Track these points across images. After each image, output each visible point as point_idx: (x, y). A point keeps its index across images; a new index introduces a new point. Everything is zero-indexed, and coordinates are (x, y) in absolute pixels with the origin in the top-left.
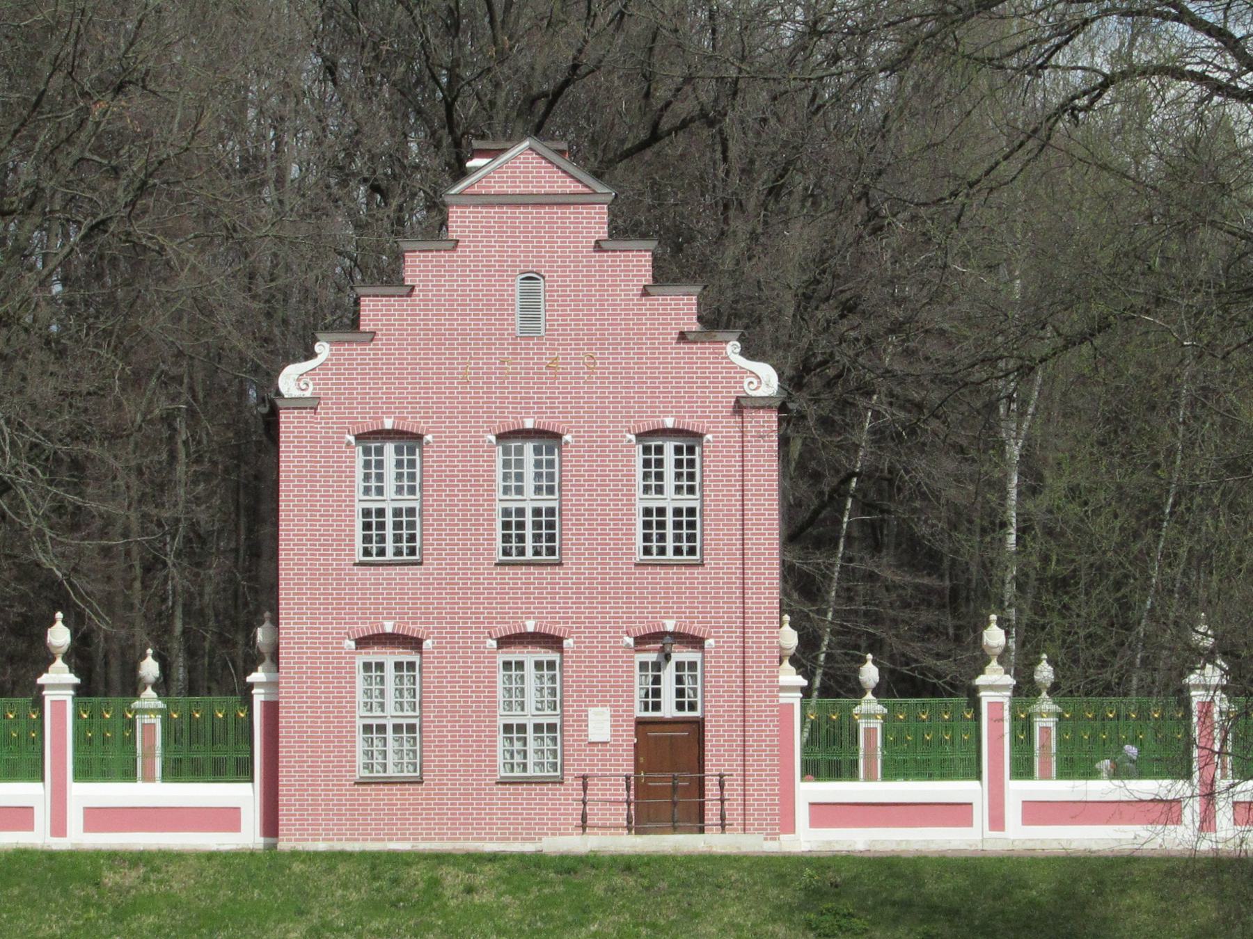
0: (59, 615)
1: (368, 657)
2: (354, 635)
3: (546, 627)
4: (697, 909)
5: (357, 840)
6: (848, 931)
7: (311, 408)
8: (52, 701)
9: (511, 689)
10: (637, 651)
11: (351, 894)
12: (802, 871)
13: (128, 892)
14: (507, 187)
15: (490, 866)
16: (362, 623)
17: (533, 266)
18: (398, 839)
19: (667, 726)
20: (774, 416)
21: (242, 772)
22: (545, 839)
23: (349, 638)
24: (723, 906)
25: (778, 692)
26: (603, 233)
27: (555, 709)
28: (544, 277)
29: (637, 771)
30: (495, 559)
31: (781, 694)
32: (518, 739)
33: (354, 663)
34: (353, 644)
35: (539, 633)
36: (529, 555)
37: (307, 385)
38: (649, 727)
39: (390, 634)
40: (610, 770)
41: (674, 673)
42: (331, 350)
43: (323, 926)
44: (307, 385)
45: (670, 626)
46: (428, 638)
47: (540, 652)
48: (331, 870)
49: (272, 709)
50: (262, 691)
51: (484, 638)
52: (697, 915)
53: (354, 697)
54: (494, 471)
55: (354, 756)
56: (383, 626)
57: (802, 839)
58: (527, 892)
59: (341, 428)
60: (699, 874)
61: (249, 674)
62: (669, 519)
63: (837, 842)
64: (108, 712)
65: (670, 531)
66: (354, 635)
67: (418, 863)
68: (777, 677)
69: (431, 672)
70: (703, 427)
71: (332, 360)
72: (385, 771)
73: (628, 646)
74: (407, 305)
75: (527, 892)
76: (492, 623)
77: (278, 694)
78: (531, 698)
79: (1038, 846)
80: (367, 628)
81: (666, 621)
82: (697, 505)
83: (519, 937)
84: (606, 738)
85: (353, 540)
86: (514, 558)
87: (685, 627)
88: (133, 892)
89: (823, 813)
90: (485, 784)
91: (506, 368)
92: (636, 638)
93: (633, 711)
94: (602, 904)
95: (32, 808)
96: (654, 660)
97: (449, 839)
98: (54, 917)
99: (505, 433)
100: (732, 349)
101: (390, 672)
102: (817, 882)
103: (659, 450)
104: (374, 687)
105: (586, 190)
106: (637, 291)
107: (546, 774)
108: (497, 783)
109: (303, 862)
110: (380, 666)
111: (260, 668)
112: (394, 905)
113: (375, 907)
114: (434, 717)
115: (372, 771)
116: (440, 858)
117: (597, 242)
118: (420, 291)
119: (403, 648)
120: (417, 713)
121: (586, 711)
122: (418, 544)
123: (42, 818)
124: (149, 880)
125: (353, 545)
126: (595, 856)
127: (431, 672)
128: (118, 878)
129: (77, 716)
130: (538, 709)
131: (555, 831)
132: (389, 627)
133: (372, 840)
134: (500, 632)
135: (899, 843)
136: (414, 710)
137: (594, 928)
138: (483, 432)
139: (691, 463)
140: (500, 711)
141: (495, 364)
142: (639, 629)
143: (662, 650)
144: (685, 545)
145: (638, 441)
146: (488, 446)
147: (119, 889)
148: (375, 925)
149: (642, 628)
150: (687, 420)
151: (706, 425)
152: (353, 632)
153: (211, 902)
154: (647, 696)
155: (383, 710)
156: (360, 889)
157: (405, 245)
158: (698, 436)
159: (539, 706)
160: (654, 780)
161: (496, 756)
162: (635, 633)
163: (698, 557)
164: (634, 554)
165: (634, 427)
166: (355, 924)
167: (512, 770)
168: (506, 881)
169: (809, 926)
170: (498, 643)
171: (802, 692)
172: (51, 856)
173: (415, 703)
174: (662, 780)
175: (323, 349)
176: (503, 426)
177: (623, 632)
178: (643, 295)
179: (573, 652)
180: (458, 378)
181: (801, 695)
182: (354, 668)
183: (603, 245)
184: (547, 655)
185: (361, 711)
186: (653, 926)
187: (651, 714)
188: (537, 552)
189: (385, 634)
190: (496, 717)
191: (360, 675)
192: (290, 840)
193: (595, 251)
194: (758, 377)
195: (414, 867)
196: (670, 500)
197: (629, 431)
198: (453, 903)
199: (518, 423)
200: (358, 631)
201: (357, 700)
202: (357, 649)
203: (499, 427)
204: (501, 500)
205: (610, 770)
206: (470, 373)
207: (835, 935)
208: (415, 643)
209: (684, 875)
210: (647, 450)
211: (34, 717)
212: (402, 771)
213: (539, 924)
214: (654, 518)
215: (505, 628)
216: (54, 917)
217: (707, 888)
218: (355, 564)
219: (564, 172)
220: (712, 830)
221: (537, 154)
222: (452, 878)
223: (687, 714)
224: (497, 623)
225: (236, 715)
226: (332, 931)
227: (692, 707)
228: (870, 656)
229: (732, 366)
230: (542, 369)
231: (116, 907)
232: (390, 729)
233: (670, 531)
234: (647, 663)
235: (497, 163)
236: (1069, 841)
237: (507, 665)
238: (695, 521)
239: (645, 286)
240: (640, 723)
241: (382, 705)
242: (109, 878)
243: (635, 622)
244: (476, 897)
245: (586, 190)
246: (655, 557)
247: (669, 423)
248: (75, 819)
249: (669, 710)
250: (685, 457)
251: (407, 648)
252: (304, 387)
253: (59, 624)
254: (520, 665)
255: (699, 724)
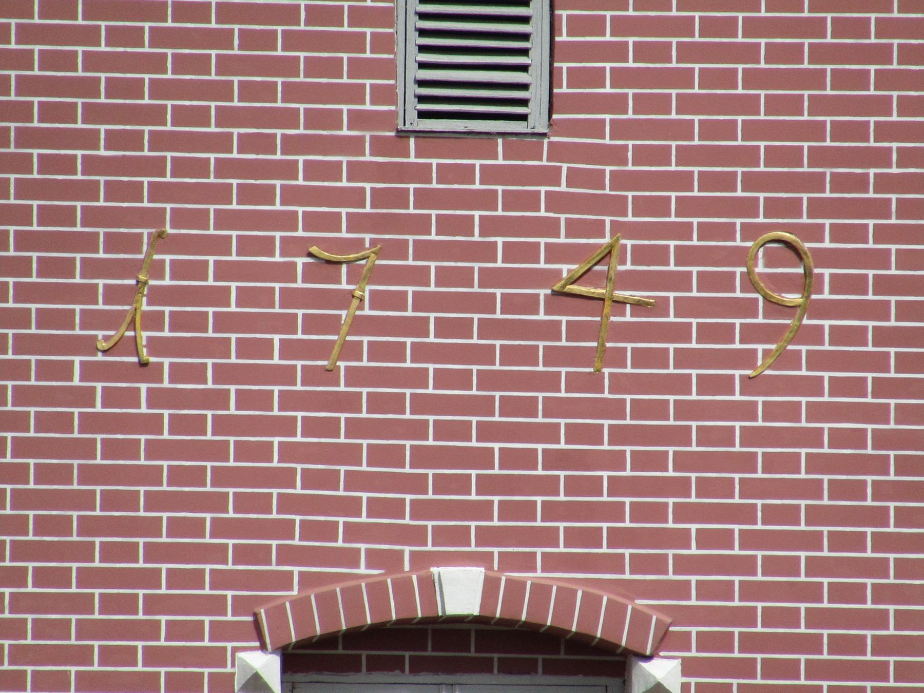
91: (343, 300)
99: (329, 640)
138: (219, 632)
141: (286, 271)
176: (326, 601)
180: (87, 345)
199: (403, 588)
203: (301, 605)
206: (154, 321)
230: (531, 305)
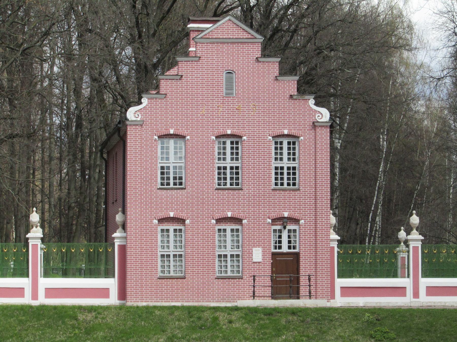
0: (35, 209)
1: (163, 227)
2: (215, 218)
3: (236, 215)
4: (324, 329)
5: (159, 301)
6: (388, 338)
7: (140, 125)
8: (413, 247)
9: (221, 240)
10: (272, 225)
11: (182, 323)
12: (364, 314)
13: (90, 323)
14: (220, 35)
15: (236, 312)
16: (161, 213)
17: (230, 68)
18: (175, 301)
19: (284, 256)
20: (328, 130)
21: (109, 274)
22: (238, 301)
23: (156, 219)
24: (335, 328)
25: (330, 242)
26: (259, 54)
27: (239, 248)
28: (235, 72)
29: (272, 273)
30: (215, 187)
31: (331, 243)
32: (224, 261)
33: (157, 229)
34: (157, 221)
35: (233, 217)
36: (228, 186)
37: (138, 115)
38: (277, 256)
39: (172, 217)
40: (262, 273)
41: (287, 234)
42: (148, 101)
43: (173, 336)
44: (138, 115)
45: (286, 215)
46: (188, 219)
47: (233, 225)
48: (172, 314)
49: (123, 249)
50: (118, 241)
51: (211, 219)
52: (324, 332)
53: (157, 243)
54: (215, 151)
55: (157, 268)
56: (169, 214)
57: (338, 302)
58: (254, 322)
59: (152, 133)
60: (322, 316)
61: (113, 234)
62: (285, 171)
63: (352, 303)
64: (64, 249)
65: (285, 176)
66: (157, 218)
67: (207, 310)
68: (329, 236)
69: (189, 233)
70: (299, 134)
71: (148, 105)
72: (169, 273)
73: (269, 223)
74: (179, 83)
75: (254, 322)
76: (214, 213)
77: (127, 242)
78: (229, 244)
79: (433, 304)
80: (163, 215)
81: (284, 213)
82: (296, 165)
83: (254, 341)
84: (260, 260)
85: (157, 179)
86: (222, 187)
87: (292, 215)
88: (92, 322)
89: (346, 291)
90: (211, 279)
91: (220, 109)
92: (272, 220)
93: (271, 249)
94: (286, 328)
95: (24, 288)
96: (279, 229)
97: (196, 301)
98: (61, 333)
99: (219, 136)
100: (312, 102)
101: (171, 233)
102: (372, 319)
103: (281, 143)
104: (165, 239)
105: (252, 37)
106: (272, 78)
107: (235, 275)
108: (216, 279)
109: (159, 310)
110: (168, 231)
111: (117, 231)
112: (201, 328)
113: (193, 329)
114: (190, 251)
115: (164, 274)
116: (216, 309)
117: (257, 58)
118: (185, 77)
119: (177, 223)
120: (183, 250)
121: (252, 249)
122: (240, 181)
123: (28, 292)
124: (98, 317)
125: (157, 181)
126: (278, 308)
127: (189, 233)
128: (84, 317)
129: (423, 253)
130: (232, 248)
131: (239, 298)
132: (172, 215)
133: (165, 302)
134: (217, 217)
135: (377, 303)
136: (181, 249)
137: (284, 337)
139: (237, 149)
140: (217, 249)
142: (274, 216)
143: (283, 224)
144: (291, 182)
145: (273, 139)
146: (212, 141)
147: (85, 321)
148: (194, 336)
149: (274, 215)
150: (293, 131)
151: (301, 133)
152: (157, 217)
153: (125, 326)
154: (276, 243)
155: (169, 249)
156: (185, 321)
157: (178, 59)
158: (240, 137)
159: (232, 247)
160: (279, 277)
161: (215, 267)
162: (272, 217)
163: (297, 187)
164: (271, 185)
165: (271, 134)
166: (186, 335)
167: (221, 273)
168: (245, 318)
169: (371, 336)
170: (158, 221)
171: (422, 242)
172: (31, 307)
173: (182, 246)
174: (285, 277)
175: (145, 101)
176: (219, 133)
177: (267, 217)
178: (275, 80)
179: (246, 225)
181: (337, 243)
182: (157, 231)
183: (260, 59)
184: (235, 227)
185: (160, 249)
186: (308, 337)
187: (277, 250)
188: (231, 184)
189: (170, 218)
190: (215, 251)
191: (159, 234)
192: (132, 302)
193: (256, 62)
194: (322, 114)
195: (206, 312)
196: (285, 163)
197: (270, 136)
198: (224, 327)
199: (225, 132)
200: (159, 216)
201: (158, 244)
202: (158, 223)
204: (160, 163)
205: (262, 273)
207: (383, 340)
208: (182, 221)
209: (316, 316)
210: (276, 143)
211: (24, 251)
212: (177, 274)
213: (261, 336)
214: (279, 171)
215: (219, 215)
216: (61, 333)
217: (327, 321)
218: (158, 189)
219: (243, 29)
220: (303, 298)
221: (233, 22)
222: (223, 318)
223: (292, 250)
224: (216, 213)
225: (98, 251)
226: (177, 338)
227: (294, 247)
228: (402, 228)
229: (311, 109)
230: (234, 110)
231: (86, 329)
232: (172, 256)
233: (285, 176)
234: (276, 230)
235: (216, 26)
236: (445, 303)
237: (219, 230)
238: (239, 172)
239: (276, 76)
240: (274, 254)
241: (168, 247)
242: (81, 317)
243: (272, 213)
244: (234, 325)
245: (252, 37)
246: (291, 187)
247: (286, 132)
248: (41, 293)
249: (285, 249)
250: (235, 146)
251: (179, 223)
252: (137, 116)
253: (35, 213)
254: (225, 230)
255: (297, 256)
